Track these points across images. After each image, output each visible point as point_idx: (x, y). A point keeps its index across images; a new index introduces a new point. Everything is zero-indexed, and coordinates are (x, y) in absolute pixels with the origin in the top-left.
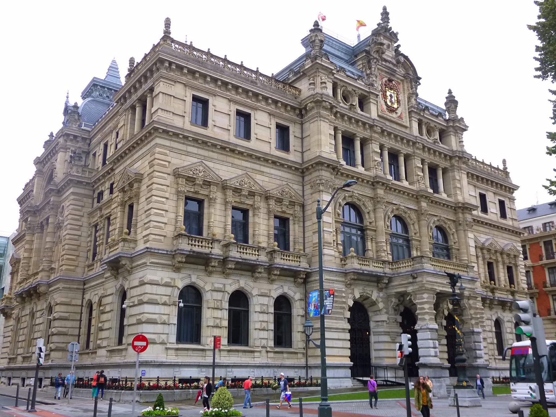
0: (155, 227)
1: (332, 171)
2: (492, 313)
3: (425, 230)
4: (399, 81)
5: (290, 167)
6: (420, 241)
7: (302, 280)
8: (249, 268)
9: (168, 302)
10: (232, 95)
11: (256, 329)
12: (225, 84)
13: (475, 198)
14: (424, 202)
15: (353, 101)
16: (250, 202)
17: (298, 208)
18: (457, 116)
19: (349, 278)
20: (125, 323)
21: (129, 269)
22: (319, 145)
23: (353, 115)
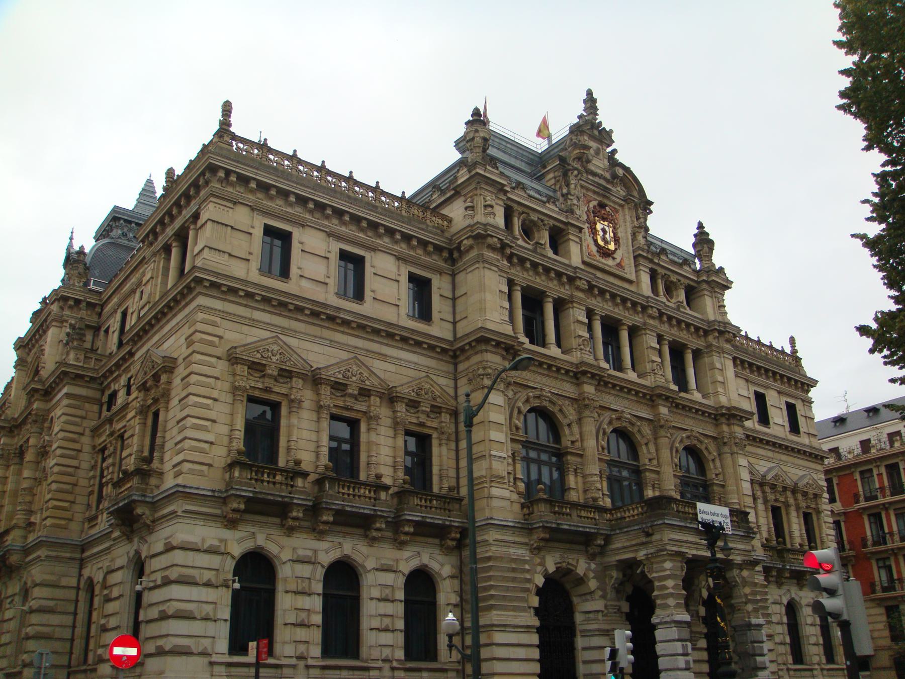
0: (192, 449)
1: (504, 353)
2: (782, 592)
3: (665, 454)
4: (616, 207)
5: (432, 348)
6: (658, 473)
7: (454, 543)
8: (359, 524)
9: (213, 580)
10: (334, 224)
11: (372, 629)
12: (321, 207)
13: (747, 400)
14: (664, 406)
15: (540, 238)
16: (361, 407)
17: (446, 417)
18: (714, 265)
19: (535, 537)
20: (141, 618)
21: (148, 522)
22: (482, 310)
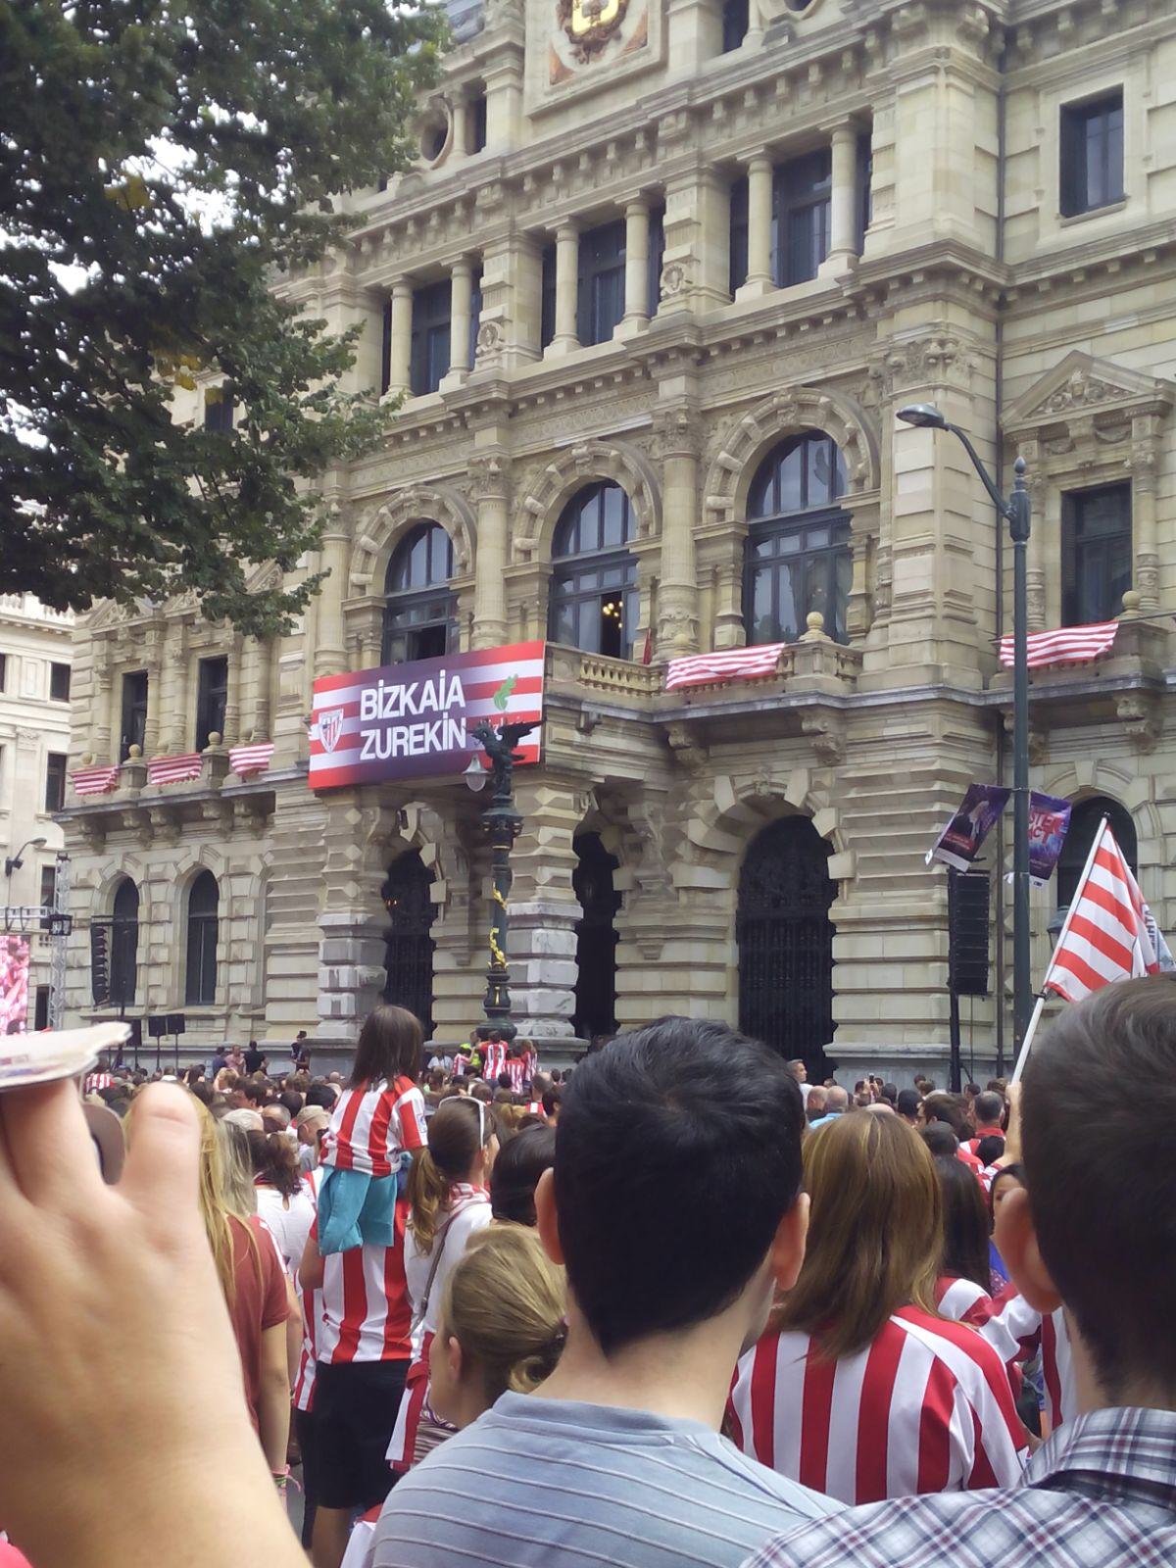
14: (671, 376)
23: (398, 212)
